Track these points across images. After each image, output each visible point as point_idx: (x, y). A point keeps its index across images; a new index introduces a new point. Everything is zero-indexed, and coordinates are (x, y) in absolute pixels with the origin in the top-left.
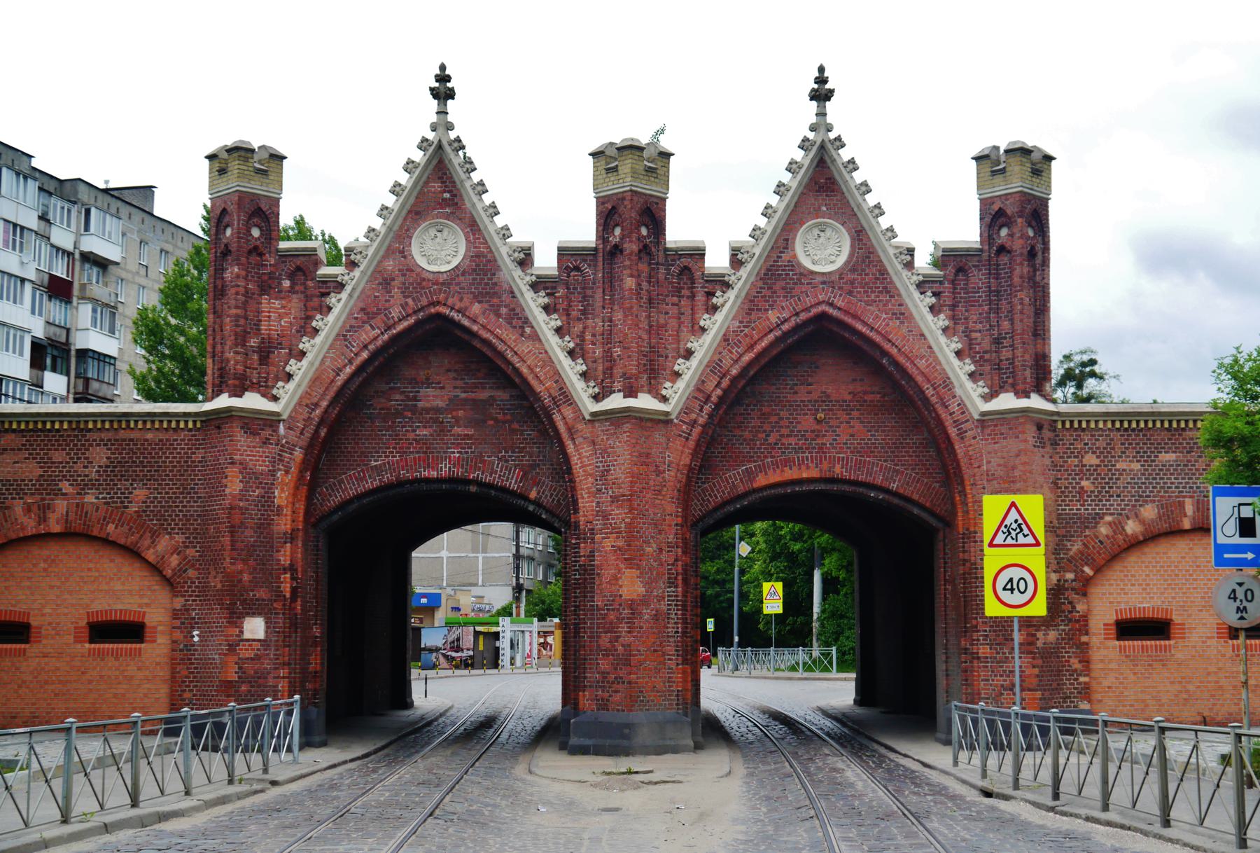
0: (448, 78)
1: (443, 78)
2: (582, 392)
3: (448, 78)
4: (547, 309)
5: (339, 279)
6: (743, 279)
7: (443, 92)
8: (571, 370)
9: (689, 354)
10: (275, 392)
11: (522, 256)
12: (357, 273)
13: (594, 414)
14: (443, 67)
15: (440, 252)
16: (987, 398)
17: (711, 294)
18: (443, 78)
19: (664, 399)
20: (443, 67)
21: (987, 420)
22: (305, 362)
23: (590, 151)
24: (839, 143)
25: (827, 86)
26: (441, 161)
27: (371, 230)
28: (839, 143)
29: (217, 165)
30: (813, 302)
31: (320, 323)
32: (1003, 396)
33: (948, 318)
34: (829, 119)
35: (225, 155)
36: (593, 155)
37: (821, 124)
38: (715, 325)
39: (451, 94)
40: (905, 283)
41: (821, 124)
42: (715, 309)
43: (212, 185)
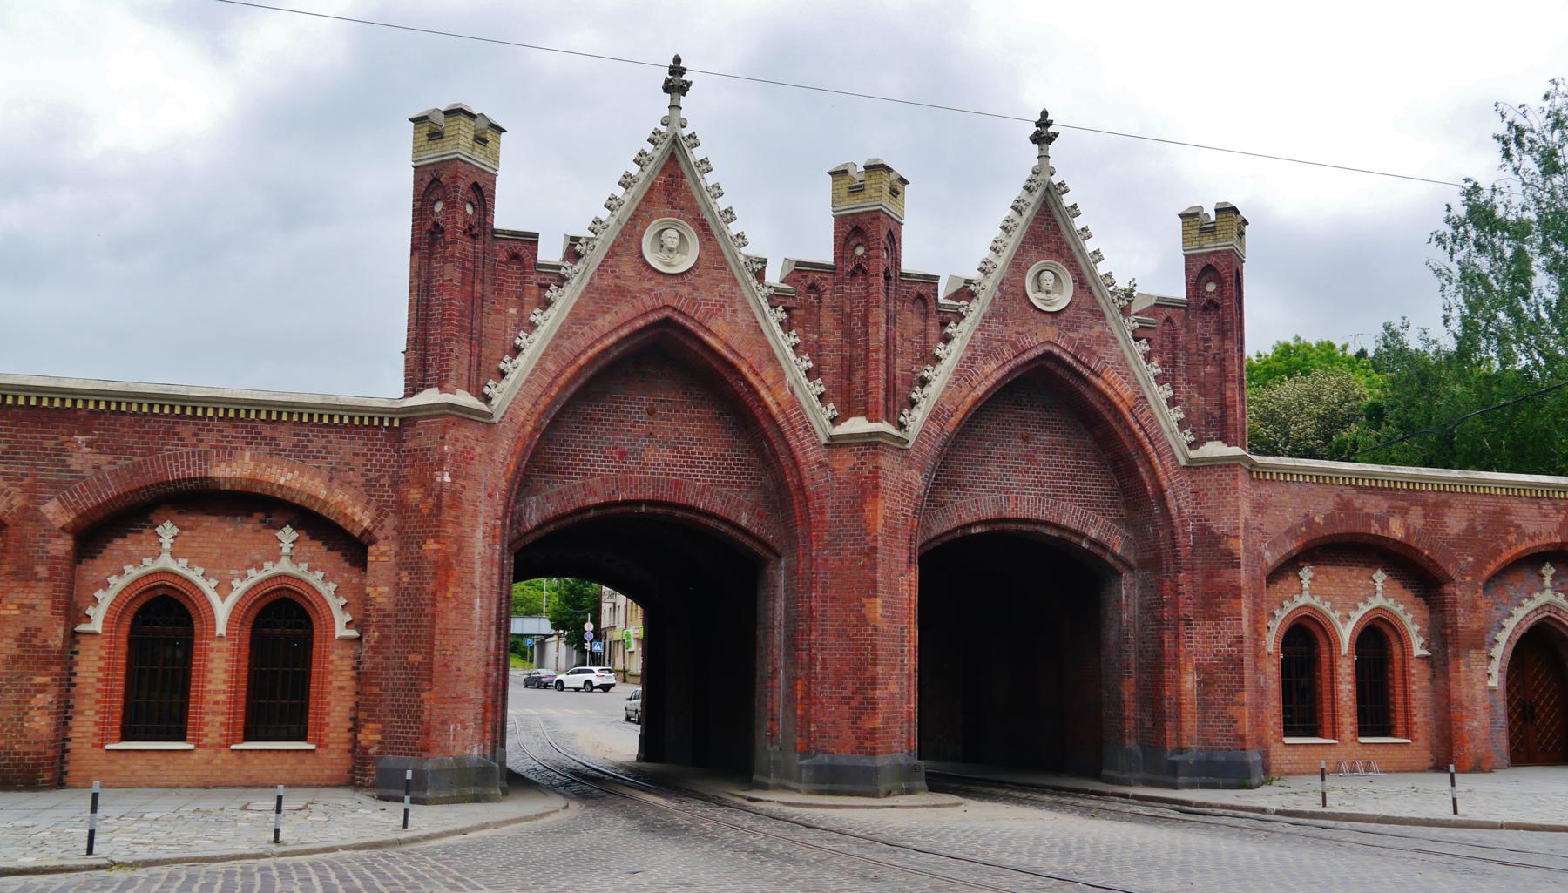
0: (682, 71)
1: (677, 69)
2: (820, 417)
3: (682, 71)
4: (786, 326)
5: (563, 271)
6: (975, 311)
7: (676, 84)
8: (808, 392)
9: (924, 382)
10: (486, 390)
11: (760, 266)
12: (579, 266)
13: (831, 438)
14: (677, 60)
15: (671, 252)
16: (1192, 445)
17: (944, 324)
18: (677, 69)
19: (901, 426)
20: (677, 60)
21: (1194, 467)
22: (521, 360)
23: (832, 168)
24: (1062, 188)
25: (1050, 129)
26: (673, 155)
27: (597, 221)
28: (1062, 188)
29: (426, 129)
30: (1039, 340)
31: (540, 318)
32: (1209, 444)
33: (1162, 365)
34: (1051, 163)
35: (441, 119)
36: (832, 173)
37: (1043, 167)
38: (951, 355)
39: (683, 88)
40: (1122, 328)
41: (1043, 167)
42: (947, 339)
43: (417, 151)
